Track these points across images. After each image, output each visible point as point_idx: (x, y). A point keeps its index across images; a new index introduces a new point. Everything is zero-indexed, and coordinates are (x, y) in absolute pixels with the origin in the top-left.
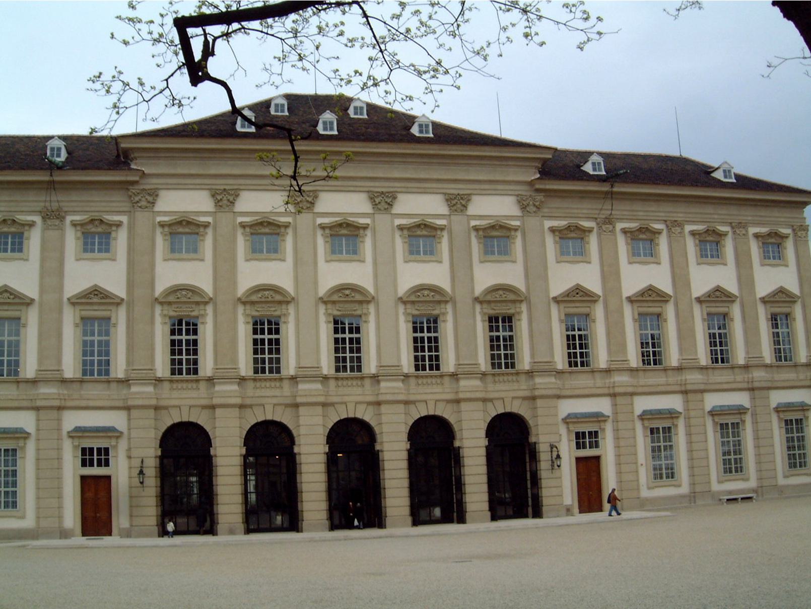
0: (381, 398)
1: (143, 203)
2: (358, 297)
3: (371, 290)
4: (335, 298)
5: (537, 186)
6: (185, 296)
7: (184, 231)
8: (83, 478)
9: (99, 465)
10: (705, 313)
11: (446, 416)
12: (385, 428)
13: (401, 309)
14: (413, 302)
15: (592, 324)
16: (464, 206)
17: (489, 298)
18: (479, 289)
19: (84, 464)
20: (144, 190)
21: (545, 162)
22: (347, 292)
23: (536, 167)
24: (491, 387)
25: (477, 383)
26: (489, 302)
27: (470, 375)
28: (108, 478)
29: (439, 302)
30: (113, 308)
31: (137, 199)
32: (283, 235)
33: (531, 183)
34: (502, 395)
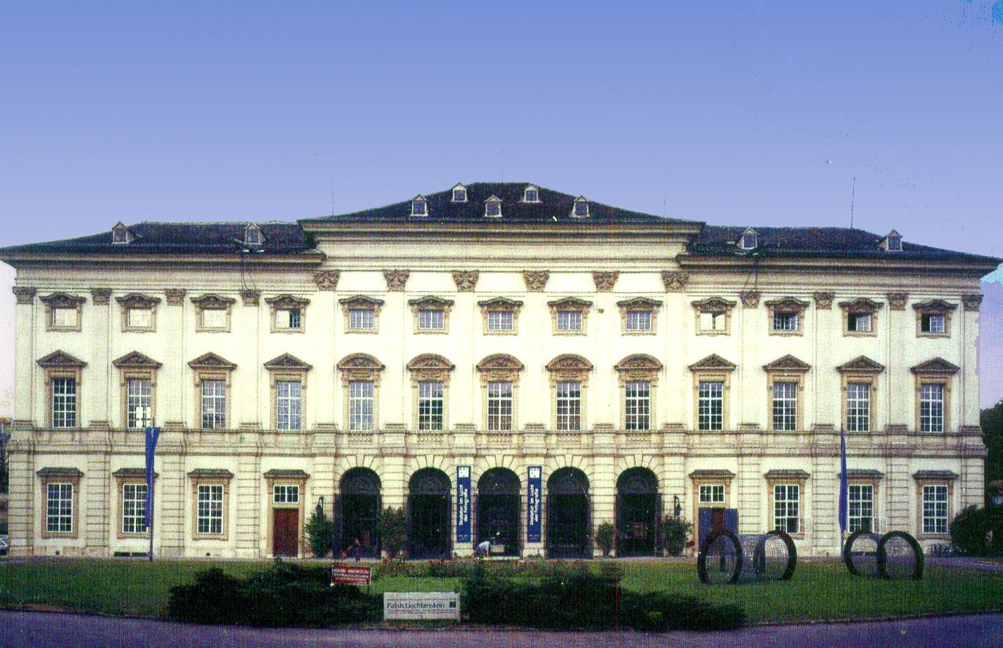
1: (326, 284)
5: (683, 263)
6: (361, 364)
7: (361, 307)
8: (277, 512)
9: (290, 500)
10: (771, 381)
11: (582, 468)
15: (801, 393)
16: (610, 284)
19: (277, 499)
20: (329, 272)
21: (693, 237)
22: (501, 361)
23: (683, 243)
28: (296, 511)
30: (303, 373)
31: (321, 279)
32: (448, 312)
33: (678, 259)
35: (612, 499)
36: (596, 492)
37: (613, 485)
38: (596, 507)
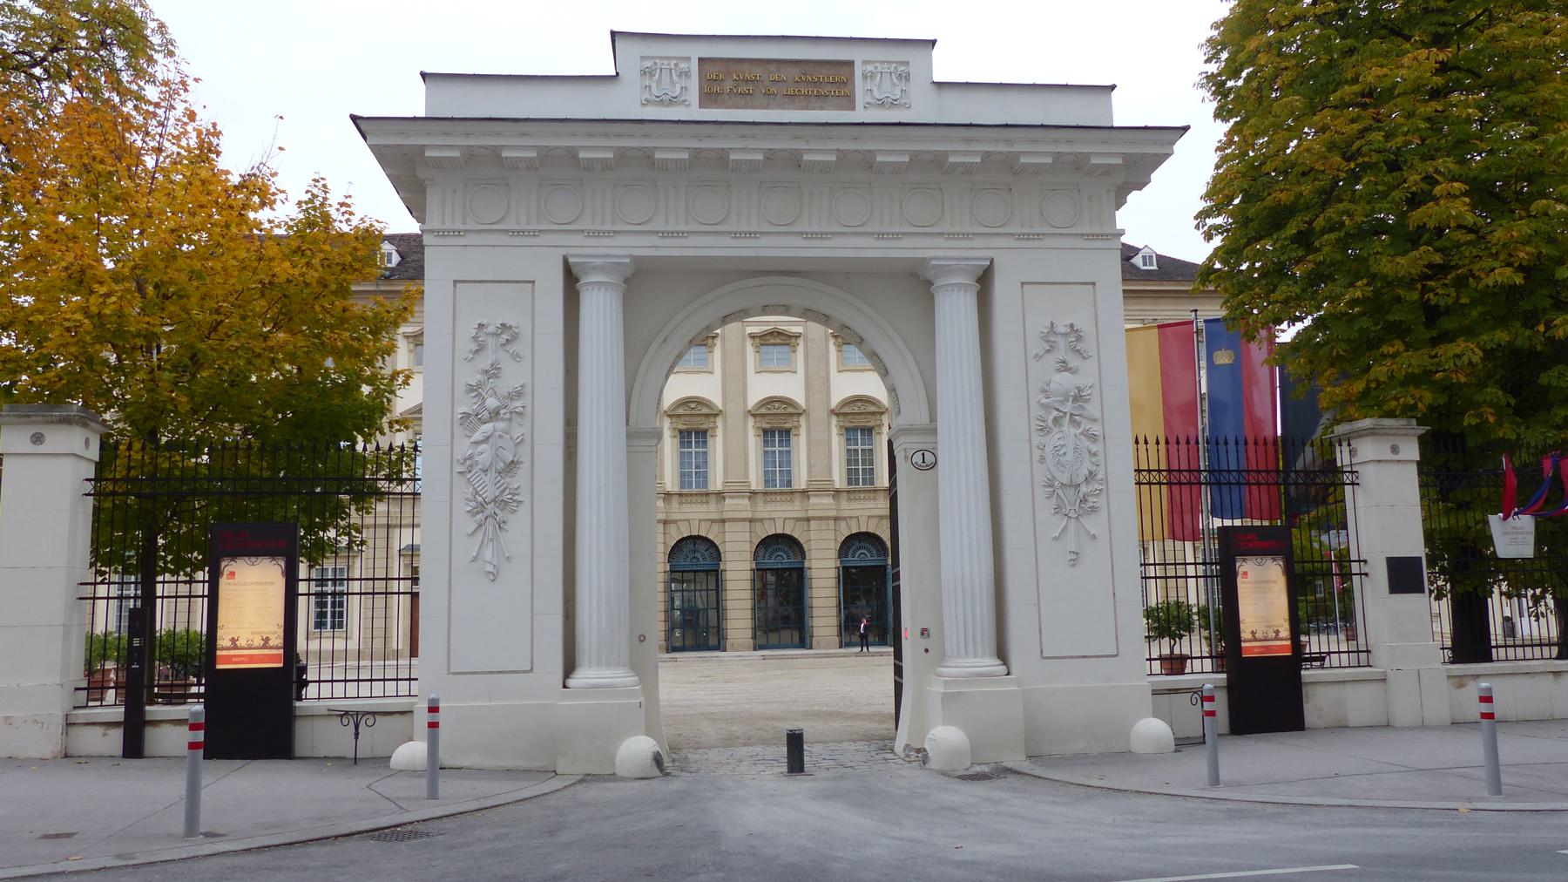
0: (725, 516)
2: (705, 411)
3: (719, 403)
4: (681, 411)
12: (728, 546)
13: (751, 421)
14: (763, 415)
17: (846, 410)
18: (835, 401)
24: (844, 504)
25: (828, 501)
26: (846, 414)
27: (822, 491)
29: (791, 415)
34: (857, 514)
35: (833, 573)
36: (814, 564)
37: (833, 554)
38: (815, 583)
